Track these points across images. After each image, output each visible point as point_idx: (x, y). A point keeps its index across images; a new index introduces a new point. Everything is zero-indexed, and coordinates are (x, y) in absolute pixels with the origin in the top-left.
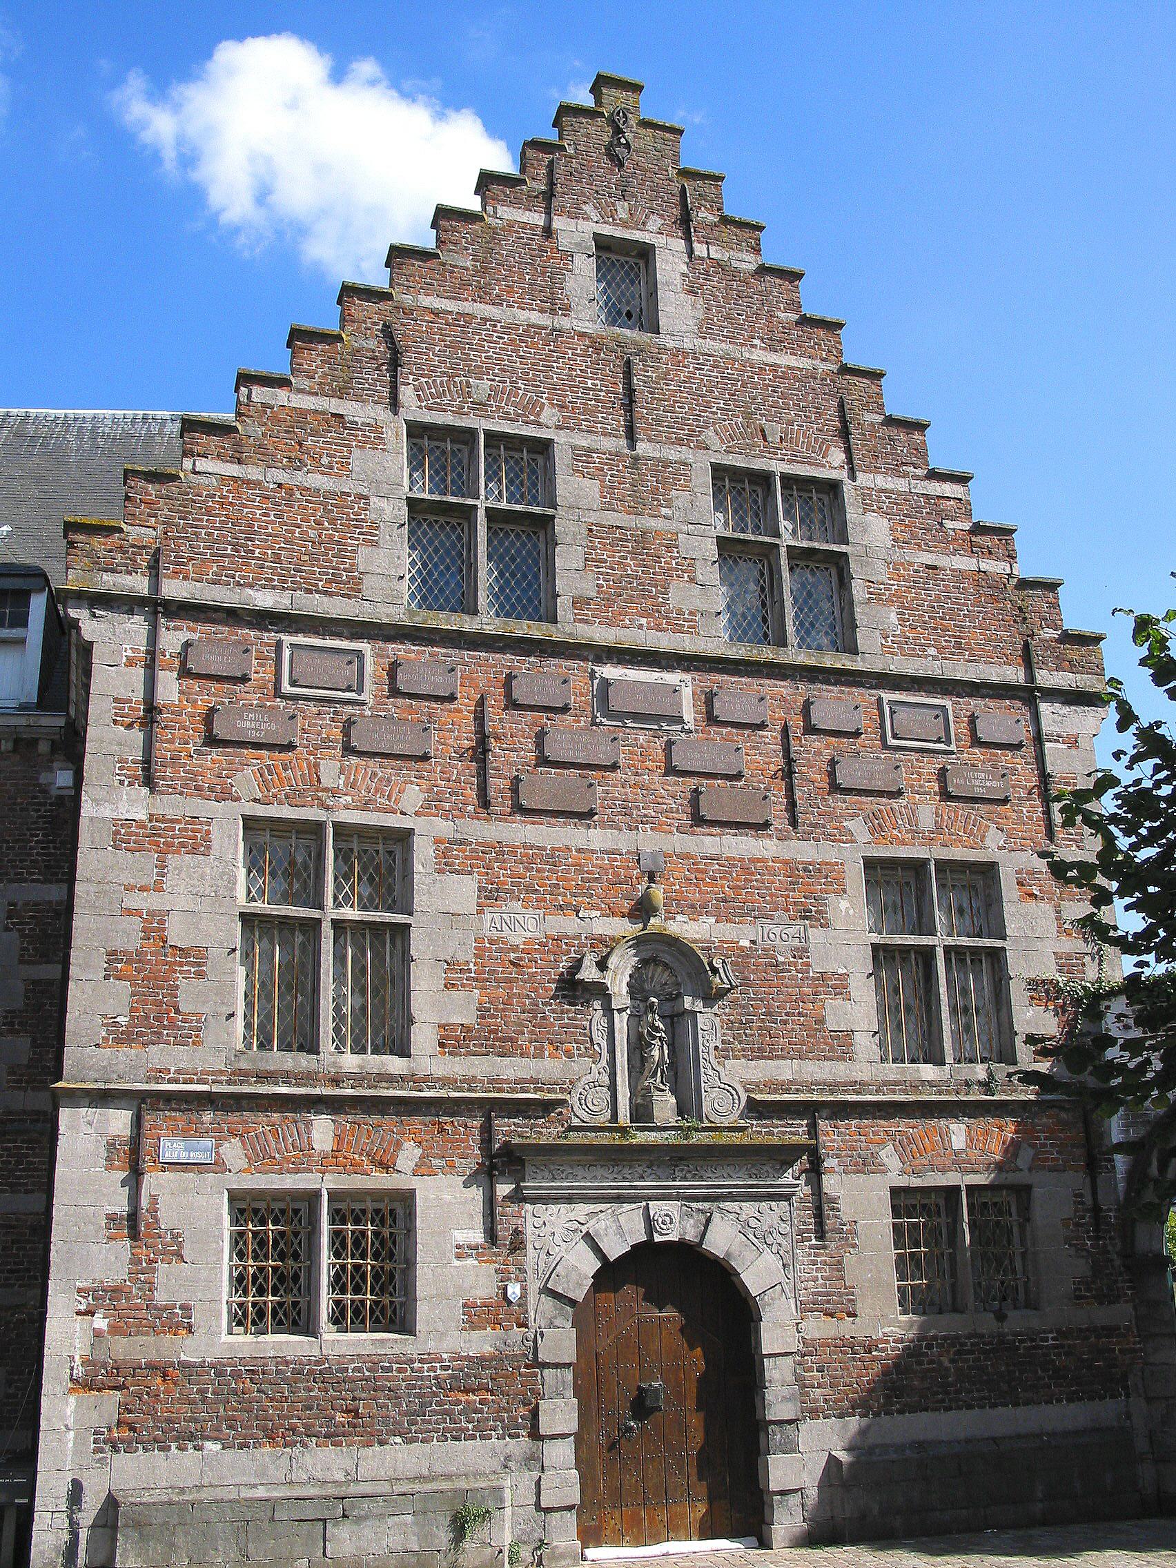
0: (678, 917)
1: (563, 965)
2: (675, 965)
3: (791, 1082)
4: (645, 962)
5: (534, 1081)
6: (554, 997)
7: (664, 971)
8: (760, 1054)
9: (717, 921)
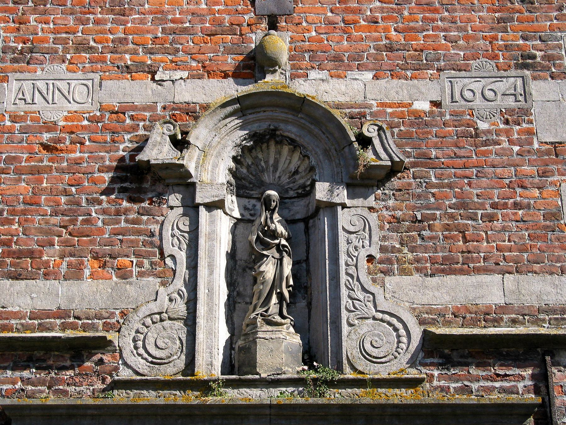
0: (313, 74)
1: (123, 148)
2: (305, 140)
3: (505, 308)
4: (259, 140)
5: (61, 314)
6: (107, 192)
7: (292, 151)
8: (447, 267)
9: (376, 77)
